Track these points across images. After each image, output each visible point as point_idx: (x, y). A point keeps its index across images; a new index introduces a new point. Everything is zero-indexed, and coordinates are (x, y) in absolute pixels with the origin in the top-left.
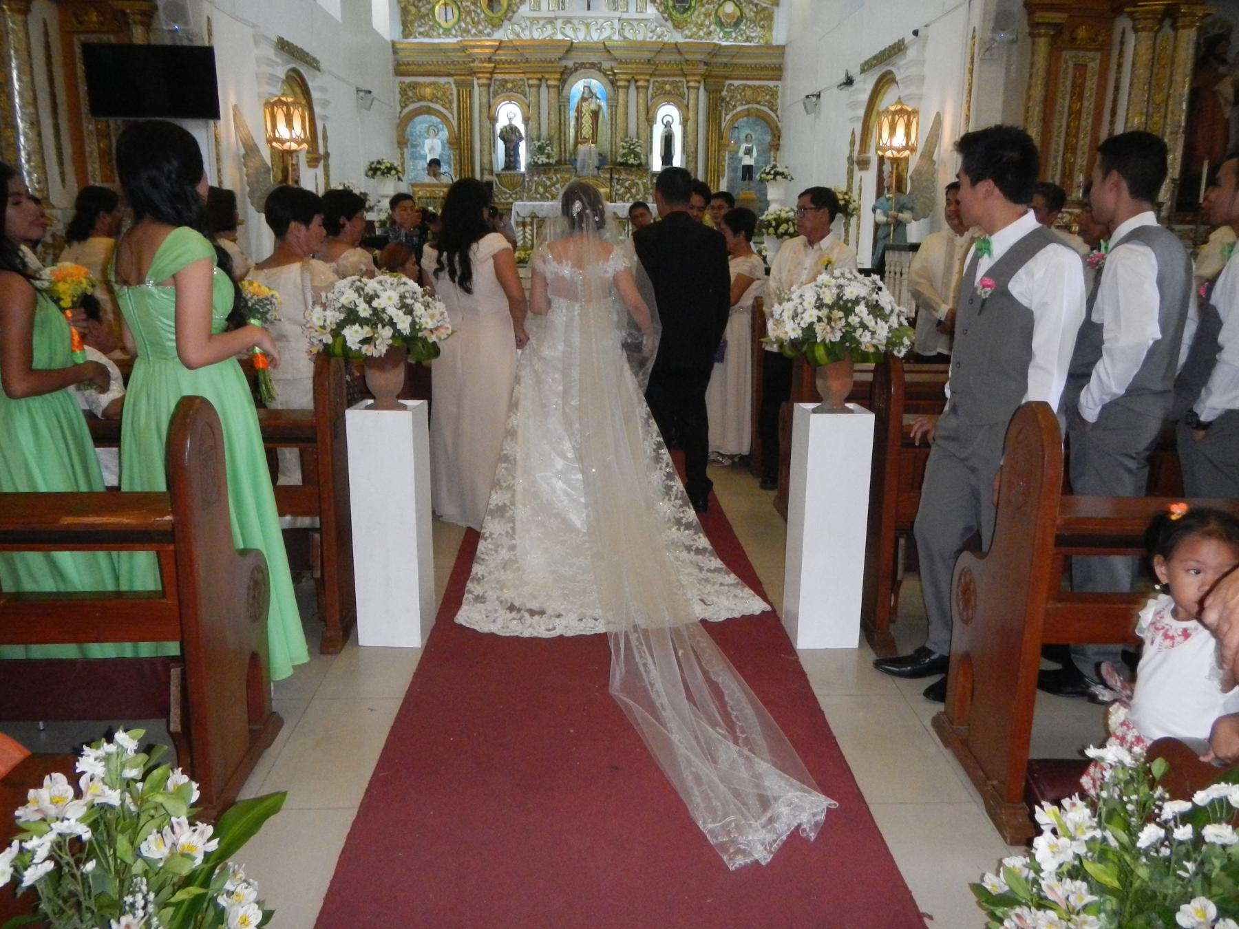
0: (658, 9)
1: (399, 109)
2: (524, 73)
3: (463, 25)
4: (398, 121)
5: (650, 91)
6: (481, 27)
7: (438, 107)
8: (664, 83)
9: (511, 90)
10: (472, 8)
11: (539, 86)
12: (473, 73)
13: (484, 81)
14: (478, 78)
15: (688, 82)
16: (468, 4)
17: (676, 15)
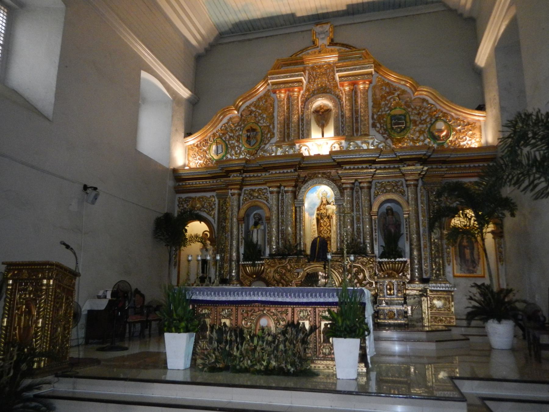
0: (378, 132)
3: (229, 156)
6: (241, 157)
10: (236, 144)
14: (231, 190)
16: (234, 142)
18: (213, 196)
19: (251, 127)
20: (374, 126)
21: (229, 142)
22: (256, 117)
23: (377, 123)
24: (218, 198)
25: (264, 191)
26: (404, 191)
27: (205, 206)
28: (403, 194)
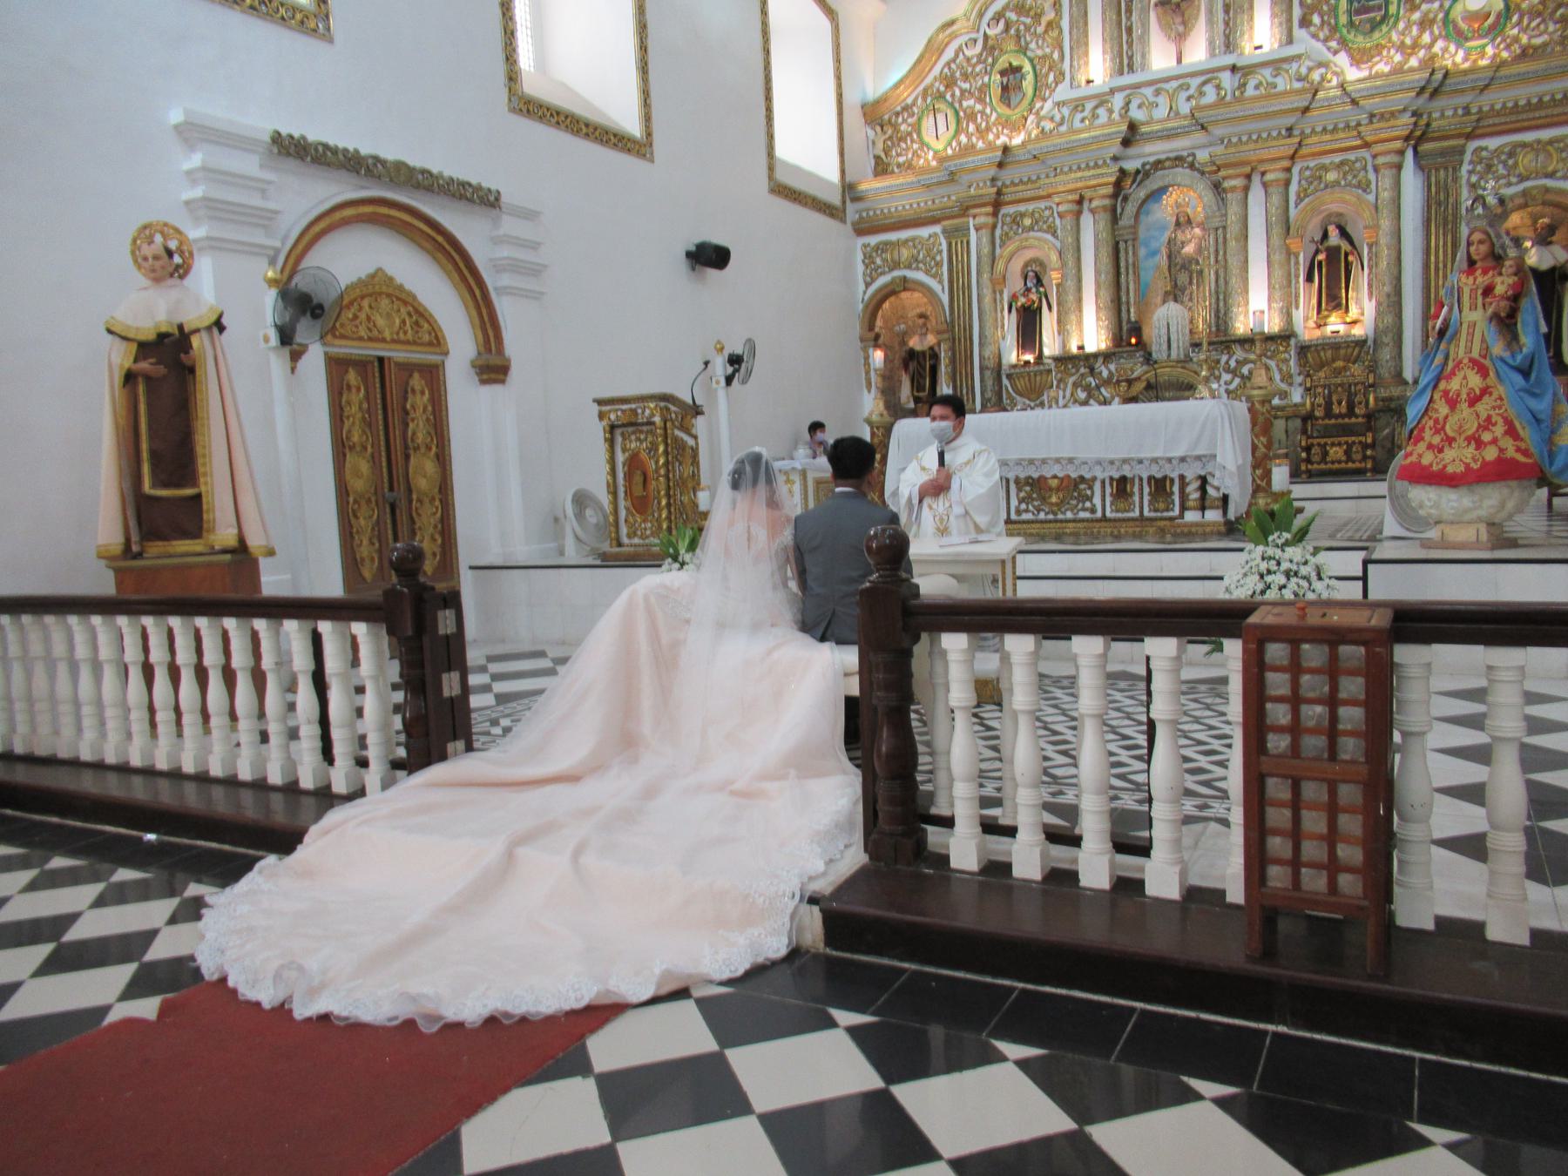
0: (1315, 36)
1: (862, 287)
2: (1049, 196)
3: (963, 139)
4: (861, 306)
5: (1293, 188)
7: (920, 276)
8: (1325, 168)
9: (1031, 228)
10: (978, 107)
11: (1079, 213)
12: (965, 210)
13: (981, 220)
14: (974, 217)
15: (1374, 157)
16: (971, 102)
17: (1359, 41)
18: (936, 234)
19: (1010, 64)
20: (1305, 22)
21: (961, 105)
22: (1018, 37)
23: (1312, 14)
24: (945, 238)
25: (1047, 213)
26: (1369, 183)
27: (921, 255)
28: (1365, 191)
